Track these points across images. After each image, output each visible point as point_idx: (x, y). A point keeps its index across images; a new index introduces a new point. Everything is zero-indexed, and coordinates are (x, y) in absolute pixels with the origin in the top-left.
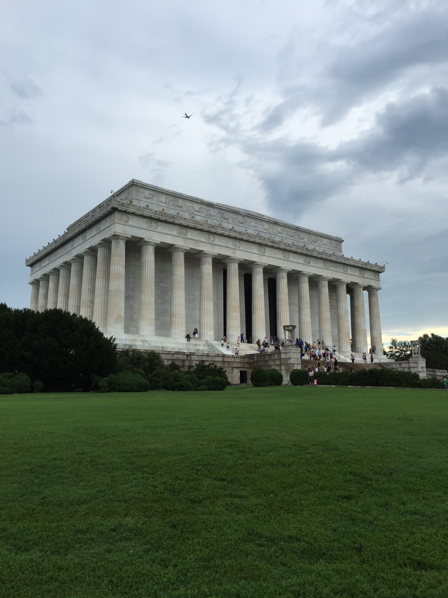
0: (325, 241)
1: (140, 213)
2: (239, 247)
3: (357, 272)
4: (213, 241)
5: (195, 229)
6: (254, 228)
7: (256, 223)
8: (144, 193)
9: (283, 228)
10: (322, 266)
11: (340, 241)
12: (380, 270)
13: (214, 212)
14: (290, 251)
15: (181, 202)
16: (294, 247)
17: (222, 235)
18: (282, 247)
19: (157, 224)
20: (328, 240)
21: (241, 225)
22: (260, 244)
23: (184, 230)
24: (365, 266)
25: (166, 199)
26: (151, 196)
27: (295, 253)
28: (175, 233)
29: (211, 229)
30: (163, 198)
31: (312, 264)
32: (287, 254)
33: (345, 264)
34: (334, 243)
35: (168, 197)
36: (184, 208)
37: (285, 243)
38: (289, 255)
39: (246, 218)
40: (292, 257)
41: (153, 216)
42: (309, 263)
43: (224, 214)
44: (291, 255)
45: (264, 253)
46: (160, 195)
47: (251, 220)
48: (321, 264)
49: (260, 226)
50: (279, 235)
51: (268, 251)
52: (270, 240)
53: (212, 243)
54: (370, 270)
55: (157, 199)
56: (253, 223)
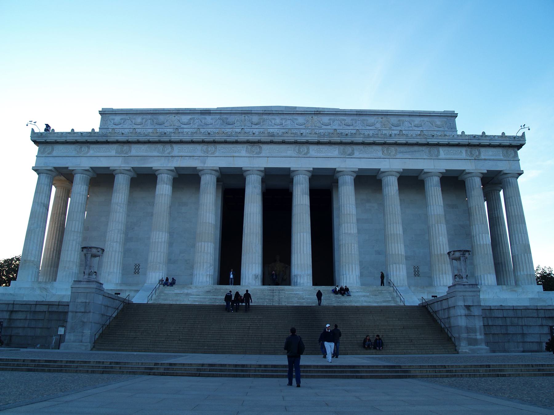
0: (417, 120)
1: (63, 139)
2: (213, 153)
3: (463, 152)
4: (169, 153)
5: (138, 142)
6: (279, 127)
7: (282, 119)
8: (114, 119)
9: (332, 117)
10: (380, 154)
11: (453, 116)
12: (514, 143)
13: (212, 119)
14: (308, 143)
15: (161, 118)
16: (315, 135)
17: (181, 142)
18: (292, 139)
19: (89, 148)
20: (426, 119)
21: (257, 127)
22: (248, 142)
23: (126, 147)
24: (475, 142)
25: (143, 119)
26: (123, 121)
27: (318, 143)
28: (113, 153)
29: (161, 138)
31: (357, 154)
32: (304, 148)
33: (428, 145)
34: (438, 121)
35: (145, 117)
36: (166, 124)
37: (296, 134)
38: (308, 149)
39: (265, 117)
40: (313, 150)
41: (80, 139)
42: (353, 153)
43: (227, 118)
44: (312, 148)
45: (260, 153)
46: (134, 117)
47: (273, 117)
48: (378, 151)
49: (289, 122)
50: (324, 127)
53: (167, 155)
54: (490, 146)
55: (130, 122)
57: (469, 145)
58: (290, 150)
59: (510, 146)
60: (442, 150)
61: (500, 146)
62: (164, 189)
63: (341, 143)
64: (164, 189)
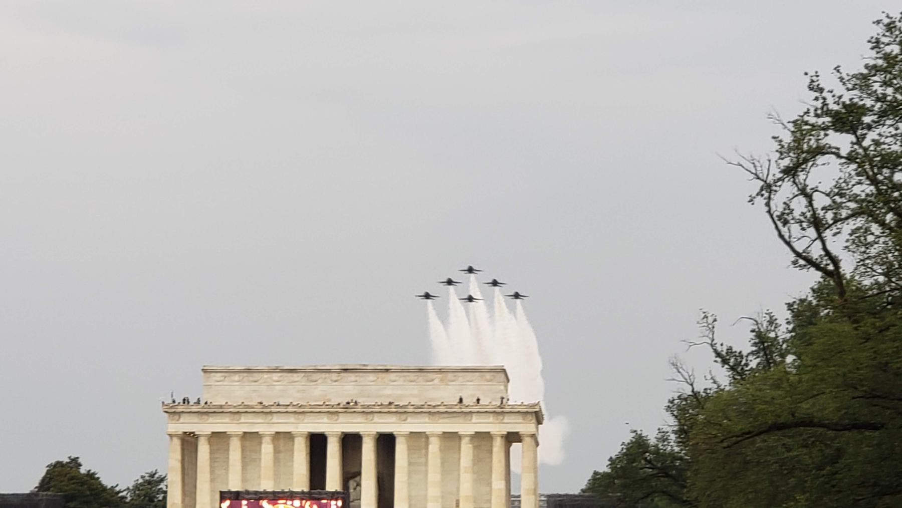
0: (469, 375)
3: (491, 418)
10: (427, 420)
15: (257, 376)
17: (279, 412)
20: (477, 374)
23: (237, 416)
30: (236, 377)
31: (409, 420)
32: (370, 417)
34: (488, 376)
40: (376, 418)
44: (376, 415)
49: (362, 379)
51: (342, 418)
52: (341, 406)
56: (352, 377)
57: (494, 412)
58: (360, 419)
59: (527, 412)
60: (474, 415)
61: (519, 412)
62: (267, 448)
63: (396, 412)
64: (267, 448)
